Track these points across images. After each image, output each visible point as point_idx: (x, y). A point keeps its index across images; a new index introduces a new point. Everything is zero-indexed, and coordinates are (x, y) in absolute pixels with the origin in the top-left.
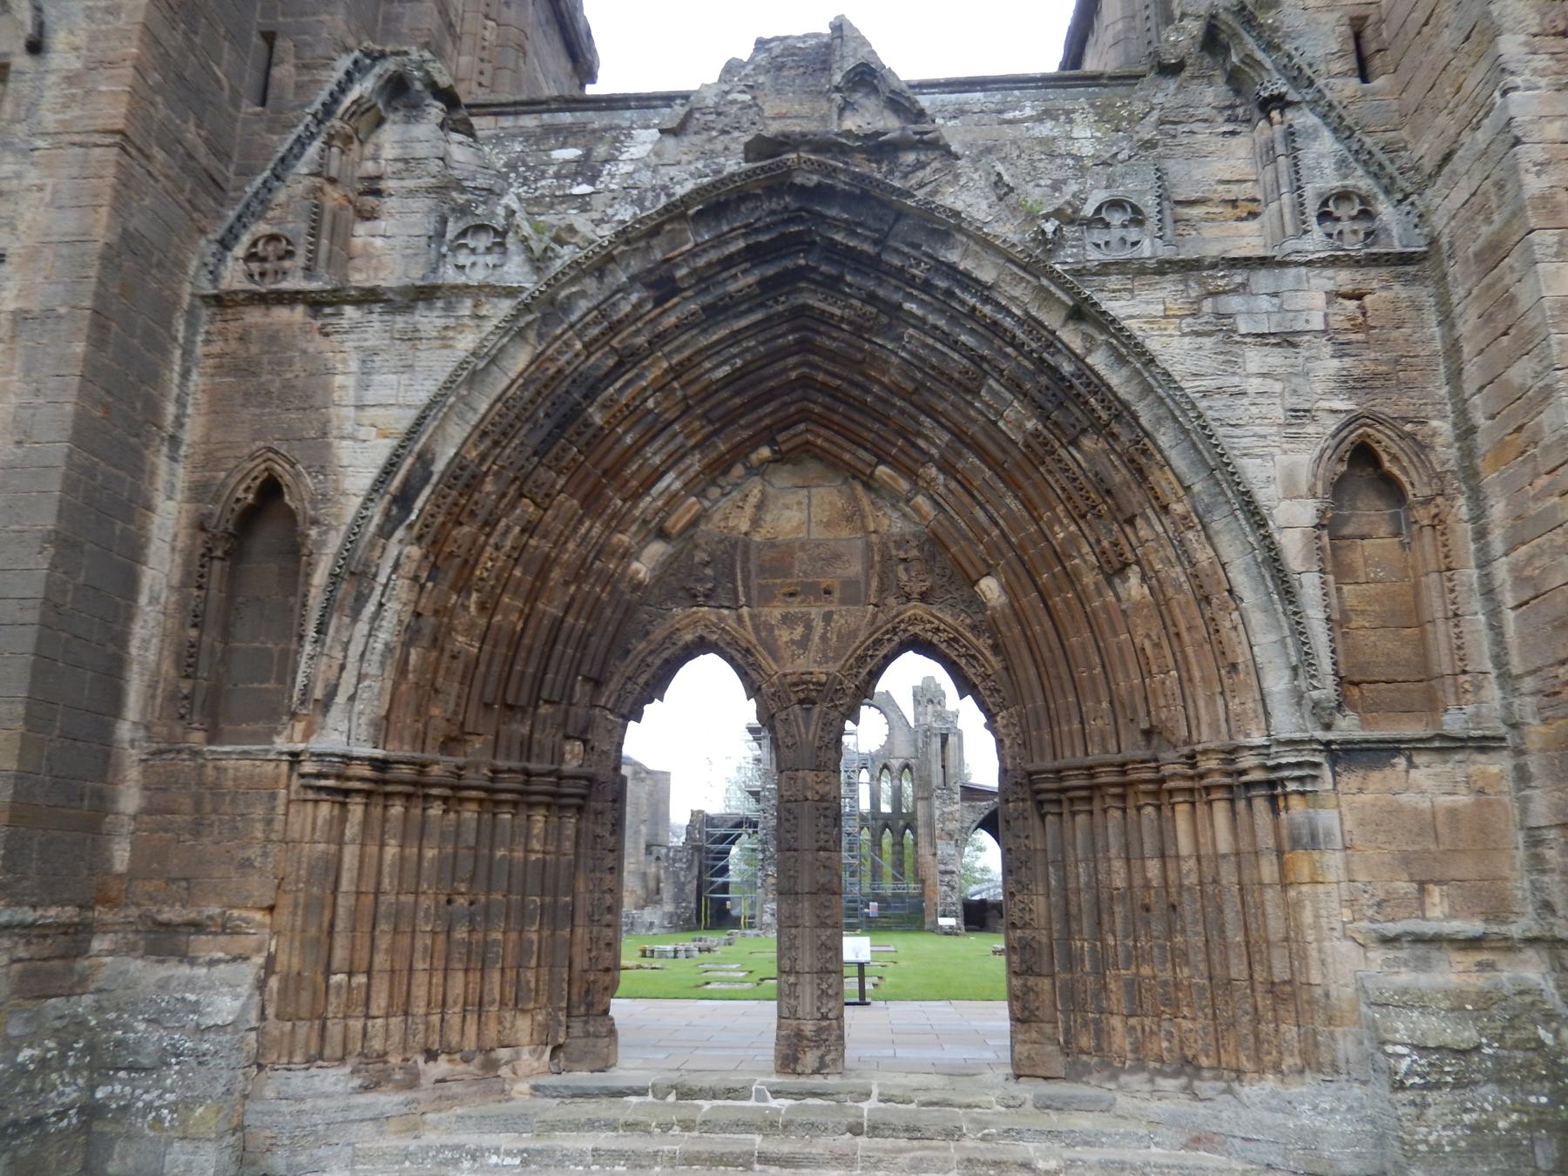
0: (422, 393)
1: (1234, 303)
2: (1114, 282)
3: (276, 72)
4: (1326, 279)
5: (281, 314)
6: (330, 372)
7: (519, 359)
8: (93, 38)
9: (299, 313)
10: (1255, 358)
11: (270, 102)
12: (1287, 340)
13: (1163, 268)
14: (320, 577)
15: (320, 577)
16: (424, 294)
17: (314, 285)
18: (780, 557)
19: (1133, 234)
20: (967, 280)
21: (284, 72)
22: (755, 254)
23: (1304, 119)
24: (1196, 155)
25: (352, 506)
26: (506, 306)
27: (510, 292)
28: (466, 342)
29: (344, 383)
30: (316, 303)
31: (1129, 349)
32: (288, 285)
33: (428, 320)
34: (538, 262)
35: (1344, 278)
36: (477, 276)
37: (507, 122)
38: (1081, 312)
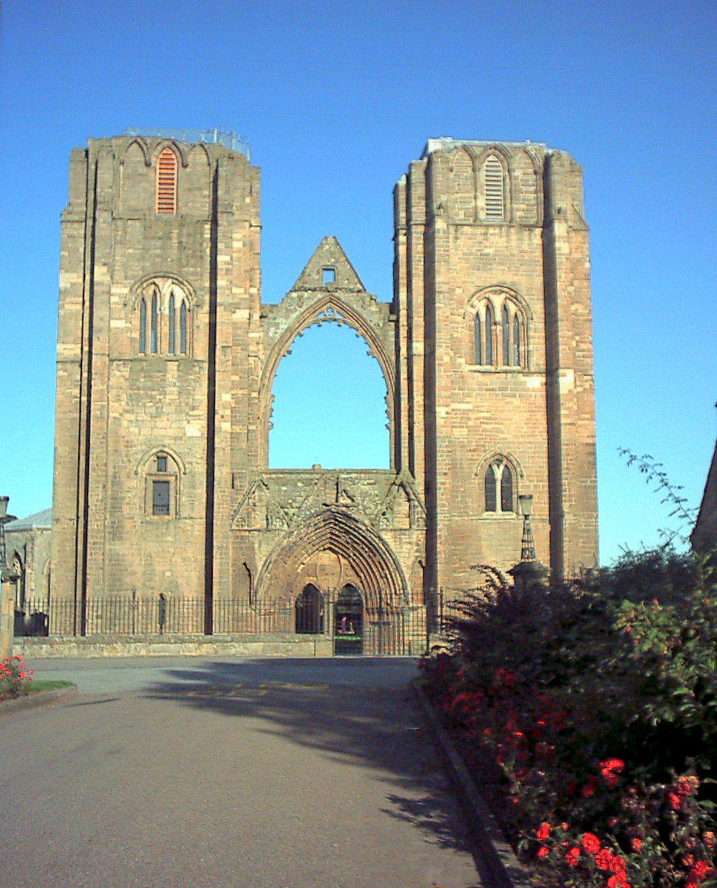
0: (270, 549)
1: (403, 537)
2: (383, 532)
3: (235, 482)
4: (416, 532)
5: (243, 533)
6: (253, 544)
7: (285, 542)
8: (222, 496)
9: (247, 533)
10: (405, 546)
11: (236, 488)
12: (410, 543)
13: (391, 530)
14: (256, 581)
15: (256, 581)
16: (268, 530)
17: (250, 529)
18: (323, 568)
19: (388, 523)
20: (361, 529)
21: (237, 483)
22: (324, 521)
23: (416, 503)
24: (400, 505)
25: (260, 568)
26: (283, 533)
27: (285, 531)
28: (277, 539)
29: (256, 546)
30: (250, 531)
31: (385, 544)
32: (246, 528)
33: (269, 535)
34: (289, 526)
35: (419, 532)
36: (278, 527)
37: (268, 476)
38: (379, 537)
